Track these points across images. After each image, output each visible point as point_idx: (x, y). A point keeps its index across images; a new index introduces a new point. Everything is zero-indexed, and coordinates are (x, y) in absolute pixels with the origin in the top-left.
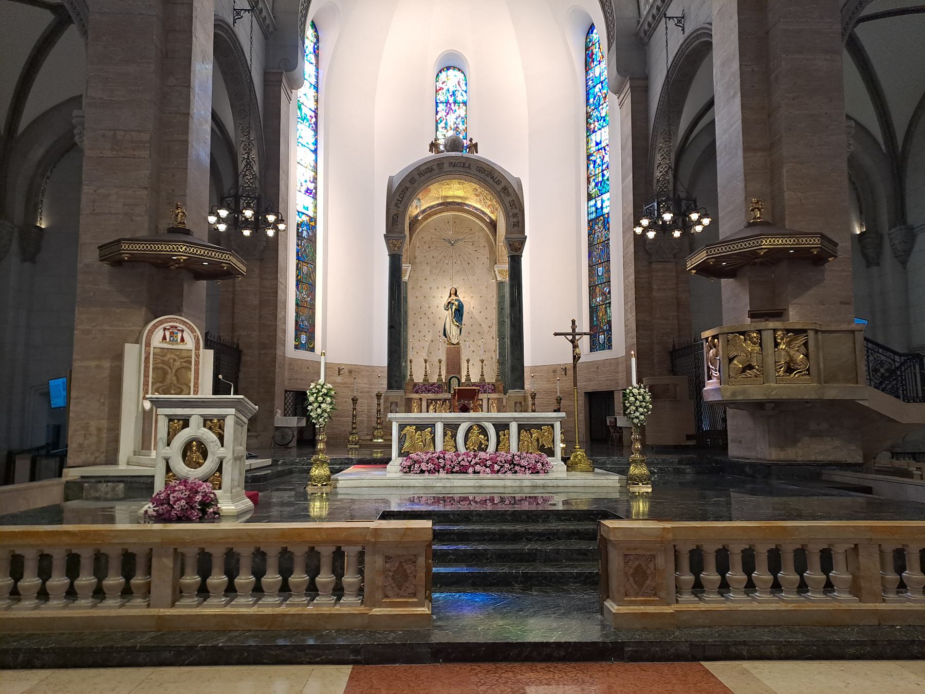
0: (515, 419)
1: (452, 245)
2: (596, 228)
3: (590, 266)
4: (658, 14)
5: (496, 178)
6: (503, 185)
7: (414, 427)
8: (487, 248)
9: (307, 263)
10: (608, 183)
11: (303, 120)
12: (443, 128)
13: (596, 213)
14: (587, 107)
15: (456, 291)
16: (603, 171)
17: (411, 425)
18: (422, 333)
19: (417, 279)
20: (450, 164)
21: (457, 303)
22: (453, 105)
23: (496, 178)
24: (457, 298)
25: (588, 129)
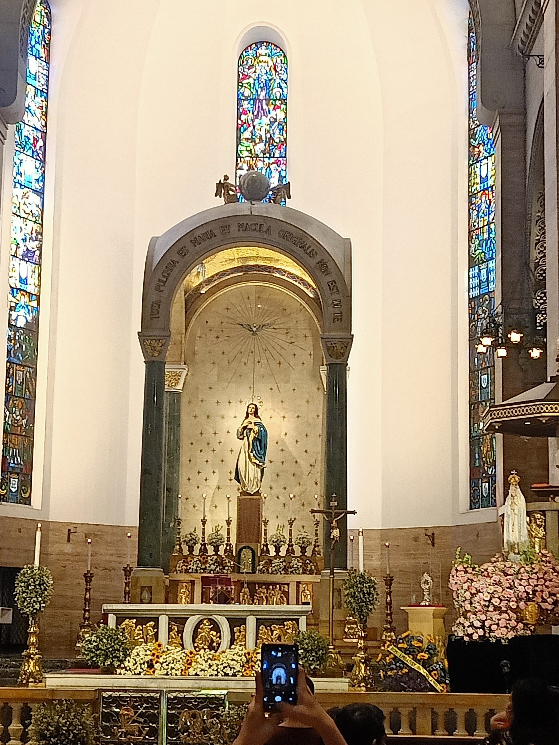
0: (252, 613)
1: (254, 333)
2: (480, 312)
4: (530, 34)
5: (310, 247)
6: (318, 258)
7: (134, 621)
8: (310, 339)
9: (24, 366)
11: (24, 148)
12: (247, 139)
14: (469, 120)
15: (257, 409)
16: (489, 224)
17: (130, 618)
18: (203, 475)
19: (197, 388)
20: (240, 225)
21: (256, 428)
22: (264, 102)
23: (310, 247)
24: (258, 420)
25: (471, 155)
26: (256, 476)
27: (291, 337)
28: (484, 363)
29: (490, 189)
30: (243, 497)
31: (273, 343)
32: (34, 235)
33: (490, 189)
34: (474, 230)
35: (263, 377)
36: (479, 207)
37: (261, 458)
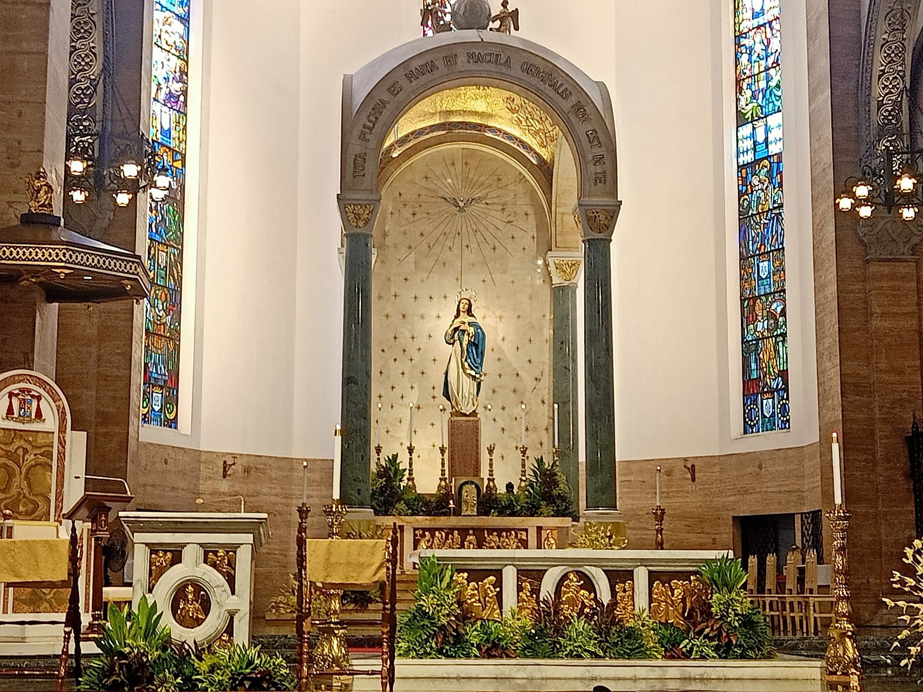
1: (461, 210)
3: (742, 258)
8: (532, 218)
10: (779, 93)
13: (755, 151)
15: (470, 305)
24: (472, 319)
26: (472, 391)
27: (509, 215)
28: (763, 247)
29: (767, 25)
30: (457, 418)
31: (485, 222)
32: (178, 74)
33: (767, 25)
34: (743, 80)
35: (473, 265)
36: (751, 49)
37: (477, 368)
